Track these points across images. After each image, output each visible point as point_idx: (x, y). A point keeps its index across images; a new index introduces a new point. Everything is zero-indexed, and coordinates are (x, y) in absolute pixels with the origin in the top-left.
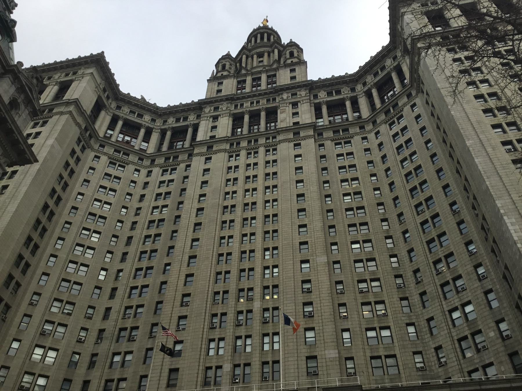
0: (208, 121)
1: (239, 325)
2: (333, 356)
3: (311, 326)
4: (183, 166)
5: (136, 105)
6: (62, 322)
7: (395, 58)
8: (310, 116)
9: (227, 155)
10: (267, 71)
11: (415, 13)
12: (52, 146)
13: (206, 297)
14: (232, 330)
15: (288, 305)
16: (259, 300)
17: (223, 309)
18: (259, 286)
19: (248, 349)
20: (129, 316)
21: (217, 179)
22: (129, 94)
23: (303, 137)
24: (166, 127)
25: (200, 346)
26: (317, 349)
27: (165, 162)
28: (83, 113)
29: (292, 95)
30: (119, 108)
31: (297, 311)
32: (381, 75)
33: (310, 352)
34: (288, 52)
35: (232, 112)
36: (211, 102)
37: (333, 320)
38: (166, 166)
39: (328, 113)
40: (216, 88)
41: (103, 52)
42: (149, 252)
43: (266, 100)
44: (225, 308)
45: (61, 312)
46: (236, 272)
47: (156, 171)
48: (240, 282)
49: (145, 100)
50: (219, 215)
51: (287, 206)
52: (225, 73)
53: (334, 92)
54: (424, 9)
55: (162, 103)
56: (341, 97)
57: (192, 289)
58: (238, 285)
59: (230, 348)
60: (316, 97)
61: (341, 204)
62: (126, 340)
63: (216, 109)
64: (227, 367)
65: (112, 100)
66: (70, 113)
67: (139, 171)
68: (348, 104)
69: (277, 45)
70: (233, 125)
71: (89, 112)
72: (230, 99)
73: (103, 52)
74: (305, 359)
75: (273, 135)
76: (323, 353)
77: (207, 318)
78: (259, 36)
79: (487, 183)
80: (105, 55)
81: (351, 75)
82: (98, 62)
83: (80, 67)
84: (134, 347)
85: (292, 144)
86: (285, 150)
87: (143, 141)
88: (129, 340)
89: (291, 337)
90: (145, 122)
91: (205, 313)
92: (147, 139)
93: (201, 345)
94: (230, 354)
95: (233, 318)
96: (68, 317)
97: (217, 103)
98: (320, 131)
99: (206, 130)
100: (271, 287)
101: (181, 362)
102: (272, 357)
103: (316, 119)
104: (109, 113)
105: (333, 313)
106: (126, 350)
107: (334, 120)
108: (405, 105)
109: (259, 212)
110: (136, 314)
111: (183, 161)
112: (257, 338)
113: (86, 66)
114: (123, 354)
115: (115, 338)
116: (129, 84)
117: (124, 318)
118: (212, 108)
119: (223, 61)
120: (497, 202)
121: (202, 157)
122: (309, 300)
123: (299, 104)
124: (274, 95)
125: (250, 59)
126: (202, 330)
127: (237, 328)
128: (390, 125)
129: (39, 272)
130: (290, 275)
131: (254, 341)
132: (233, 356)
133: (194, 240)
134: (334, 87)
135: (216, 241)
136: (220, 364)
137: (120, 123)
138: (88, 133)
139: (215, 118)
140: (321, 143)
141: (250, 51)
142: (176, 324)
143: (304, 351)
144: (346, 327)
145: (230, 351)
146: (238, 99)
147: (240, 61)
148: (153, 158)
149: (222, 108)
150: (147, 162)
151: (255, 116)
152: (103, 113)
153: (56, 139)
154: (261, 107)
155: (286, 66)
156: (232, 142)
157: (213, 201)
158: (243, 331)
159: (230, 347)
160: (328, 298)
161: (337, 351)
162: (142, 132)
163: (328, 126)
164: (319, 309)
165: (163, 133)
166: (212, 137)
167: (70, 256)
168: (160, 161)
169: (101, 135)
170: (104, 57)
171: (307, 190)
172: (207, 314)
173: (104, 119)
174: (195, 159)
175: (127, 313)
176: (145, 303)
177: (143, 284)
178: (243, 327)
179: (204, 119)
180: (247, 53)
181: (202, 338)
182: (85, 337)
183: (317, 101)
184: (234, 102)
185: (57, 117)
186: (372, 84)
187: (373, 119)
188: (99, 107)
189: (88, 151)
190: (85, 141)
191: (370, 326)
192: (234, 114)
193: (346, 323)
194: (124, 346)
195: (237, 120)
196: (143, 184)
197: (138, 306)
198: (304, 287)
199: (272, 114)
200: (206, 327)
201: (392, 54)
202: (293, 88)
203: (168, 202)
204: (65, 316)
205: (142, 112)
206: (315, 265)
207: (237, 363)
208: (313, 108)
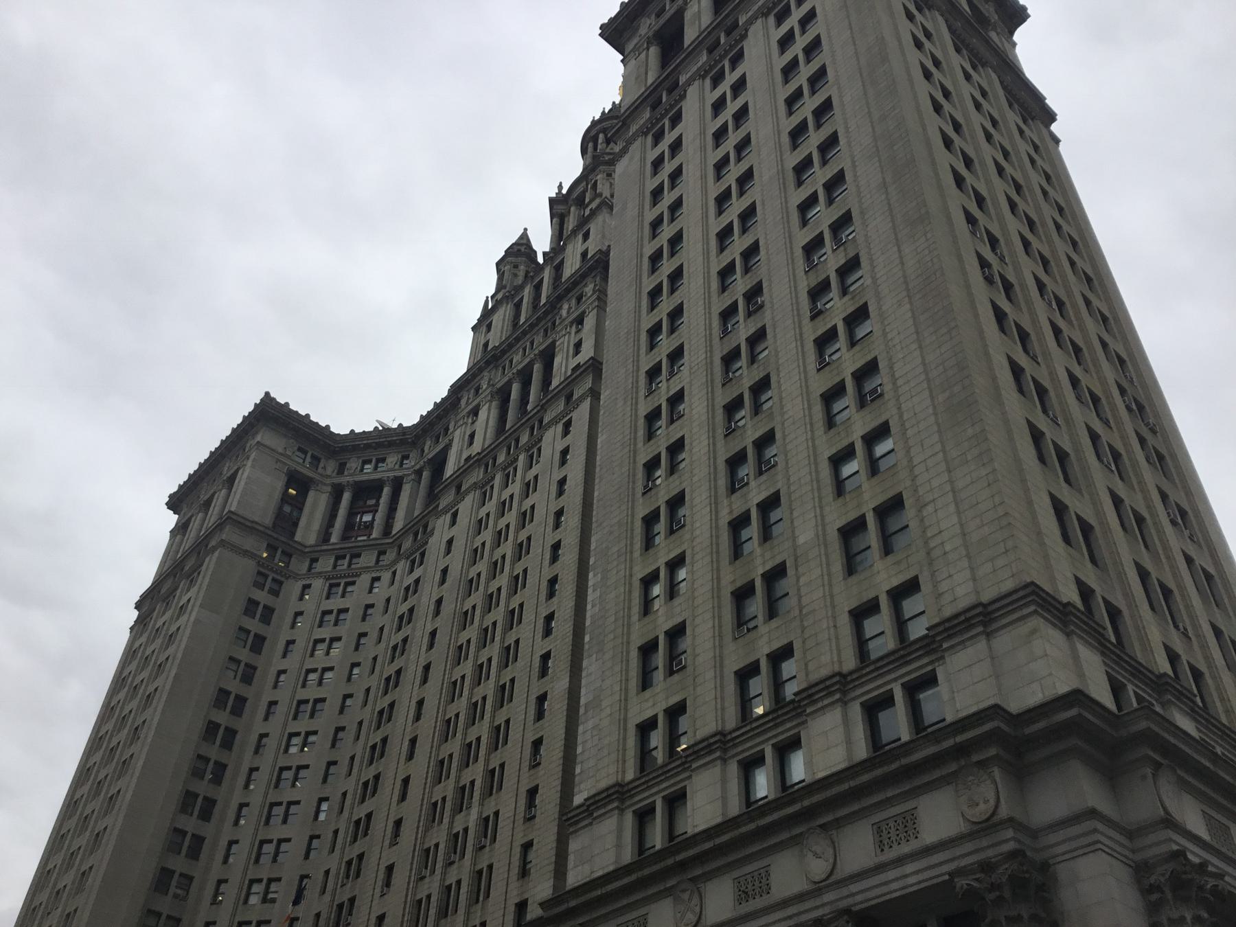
5: (368, 446)
22: (352, 431)
28: (252, 528)
30: (341, 469)
40: (482, 342)
41: (267, 394)
55: (410, 419)
66: (223, 543)
71: (268, 520)
73: (267, 394)
78: (591, 145)
82: (270, 414)
96: (271, 905)
129: (223, 843)
137: (347, 496)
139: (475, 412)
143: (515, 893)
148: (398, 543)
150: (391, 555)
152: (311, 494)
162: (386, 491)
170: (274, 399)
178: (455, 866)
192: (500, 390)
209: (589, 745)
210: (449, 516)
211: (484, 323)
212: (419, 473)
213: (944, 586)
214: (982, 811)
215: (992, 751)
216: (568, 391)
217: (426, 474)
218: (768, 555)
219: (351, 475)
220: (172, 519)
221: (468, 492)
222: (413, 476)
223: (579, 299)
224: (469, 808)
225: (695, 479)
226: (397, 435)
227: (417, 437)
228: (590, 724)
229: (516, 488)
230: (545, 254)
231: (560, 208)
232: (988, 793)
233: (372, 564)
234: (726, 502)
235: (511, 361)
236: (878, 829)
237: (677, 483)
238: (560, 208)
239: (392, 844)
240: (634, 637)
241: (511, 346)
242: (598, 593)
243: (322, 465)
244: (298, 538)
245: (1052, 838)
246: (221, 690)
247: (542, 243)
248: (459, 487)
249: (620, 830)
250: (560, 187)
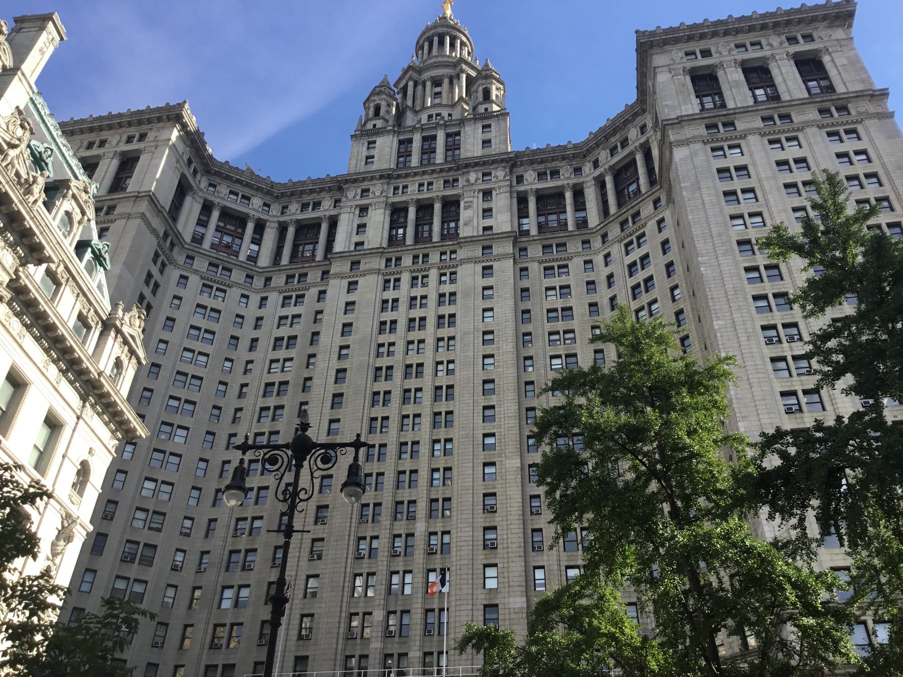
0: (352, 215)
1: (394, 555)
2: (519, 605)
3: (493, 561)
4: (313, 292)
6: (150, 542)
7: (643, 129)
8: (509, 218)
9: (381, 279)
10: (445, 126)
11: (674, 70)
13: (350, 512)
14: (385, 563)
15: (464, 530)
16: (424, 520)
17: (373, 531)
18: (425, 499)
19: (408, 590)
20: (242, 531)
21: (366, 321)
23: (498, 255)
25: (342, 584)
26: (499, 595)
27: (286, 283)
28: (160, 212)
29: (484, 175)
31: (475, 539)
32: (621, 154)
33: (490, 599)
34: (481, 88)
35: (391, 200)
36: (355, 181)
37: (522, 554)
38: (289, 291)
39: (538, 209)
40: (365, 153)
42: (267, 434)
43: (442, 182)
44: (376, 529)
45: (147, 527)
46: (392, 475)
47: (274, 298)
48: (399, 491)
49: (252, 173)
50: (369, 382)
51: (467, 377)
52: (379, 123)
53: (548, 172)
54: (689, 65)
56: (559, 183)
57: (330, 499)
58: (395, 495)
59: (382, 588)
60: (520, 180)
61: (546, 373)
62: (239, 569)
64: (378, 615)
65: (202, 175)
66: (143, 216)
67: (247, 297)
68: (568, 195)
69: (464, 67)
70: (391, 221)
72: (386, 176)
74: (482, 607)
75: (452, 248)
76: (506, 600)
77: (351, 543)
78: (436, 39)
79: (732, 393)
81: (576, 146)
83: (150, 126)
84: (251, 578)
85: (479, 268)
86: (469, 276)
87: (252, 242)
88: (243, 569)
89: (465, 577)
90: (254, 210)
91: (349, 536)
93: (344, 582)
94: (382, 597)
95: (387, 545)
97: (366, 183)
99: (349, 230)
100: (441, 501)
101: (317, 605)
102: (439, 603)
103: (520, 218)
104: (198, 199)
105: (522, 545)
106: (241, 583)
107: (547, 221)
108: (649, 218)
109: (427, 382)
110: (251, 529)
111: (315, 285)
112: (420, 575)
113: (161, 124)
114: (236, 588)
115: (224, 563)
117: (235, 536)
118: (359, 191)
119: (375, 98)
120: (740, 424)
121: (343, 280)
122: (492, 524)
123: (494, 193)
124: (455, 173)
125: (420, 87)
126: (344, 560)
127: (392, 559)
128: (627, 246)
130: (467, 484)
131: (416, 580)
132: (386, 600)
133: (331, 421)
134: (549, 165)
135: (364, 425)
136: (370, 610)
137: (216, 214)
138: (169, 241)
139: (364, 210)
140: (524, 265)
141: (420, 71)
142: (308, 550)
143: (482, 596)
144: (540, 564)
145: (383, 592)
146: (399, 177)
147: (404, 90)
148: (268, 275)
149: (374, 193)
151: (425, 208)
152: (188, 200)
153: (124, 264)
154: (435, 195)
155: (476, 117)
156: (388, 256)
157: (361, 359)
158: (401, 563)
159: (383, 587)
160: (517, 522)
161: (525, 599)
162: (250, 226)
163: (535, 238)
164: (505, 537)
165: (282, 229)
166: (359, 244)
167: (154, 442)
168: (279, 280)
169: (188, 238)
171: (498, 348)
172: (352, 538)
174: (333, 282)
175: (239, 527)
176: (264, 514)
177: (260, 485)
178: (401, 558)
179: (345, 209)
180: (415, 76)
181: (345, 572)
182: (183, 562)
183: (521, 188)
184: (393, 181)
185: (122, 222)
186: (607, 167)
187: (603, 232)
188: (183, 190)
189: (169, 269)
190: (165, 255)
191: (572, 564)
192: (393, 204)
193: (540, 558)
194: (238, 577)
195: (397, 213)
196: (254, 321)
197: (254, 518)
198: (486, 503)
199: (451, 206)
200: (350, 556)
201: (639, 121)
202: (484, 164)
203: (292, 353)
204: (152, 532)
205: (247, 192)
206: (504, 470)
207: (392, 609)
208: (515, 201)
222: (276, 225)
226: (267, 185)
227: (283, 195)
233: (242, 281)
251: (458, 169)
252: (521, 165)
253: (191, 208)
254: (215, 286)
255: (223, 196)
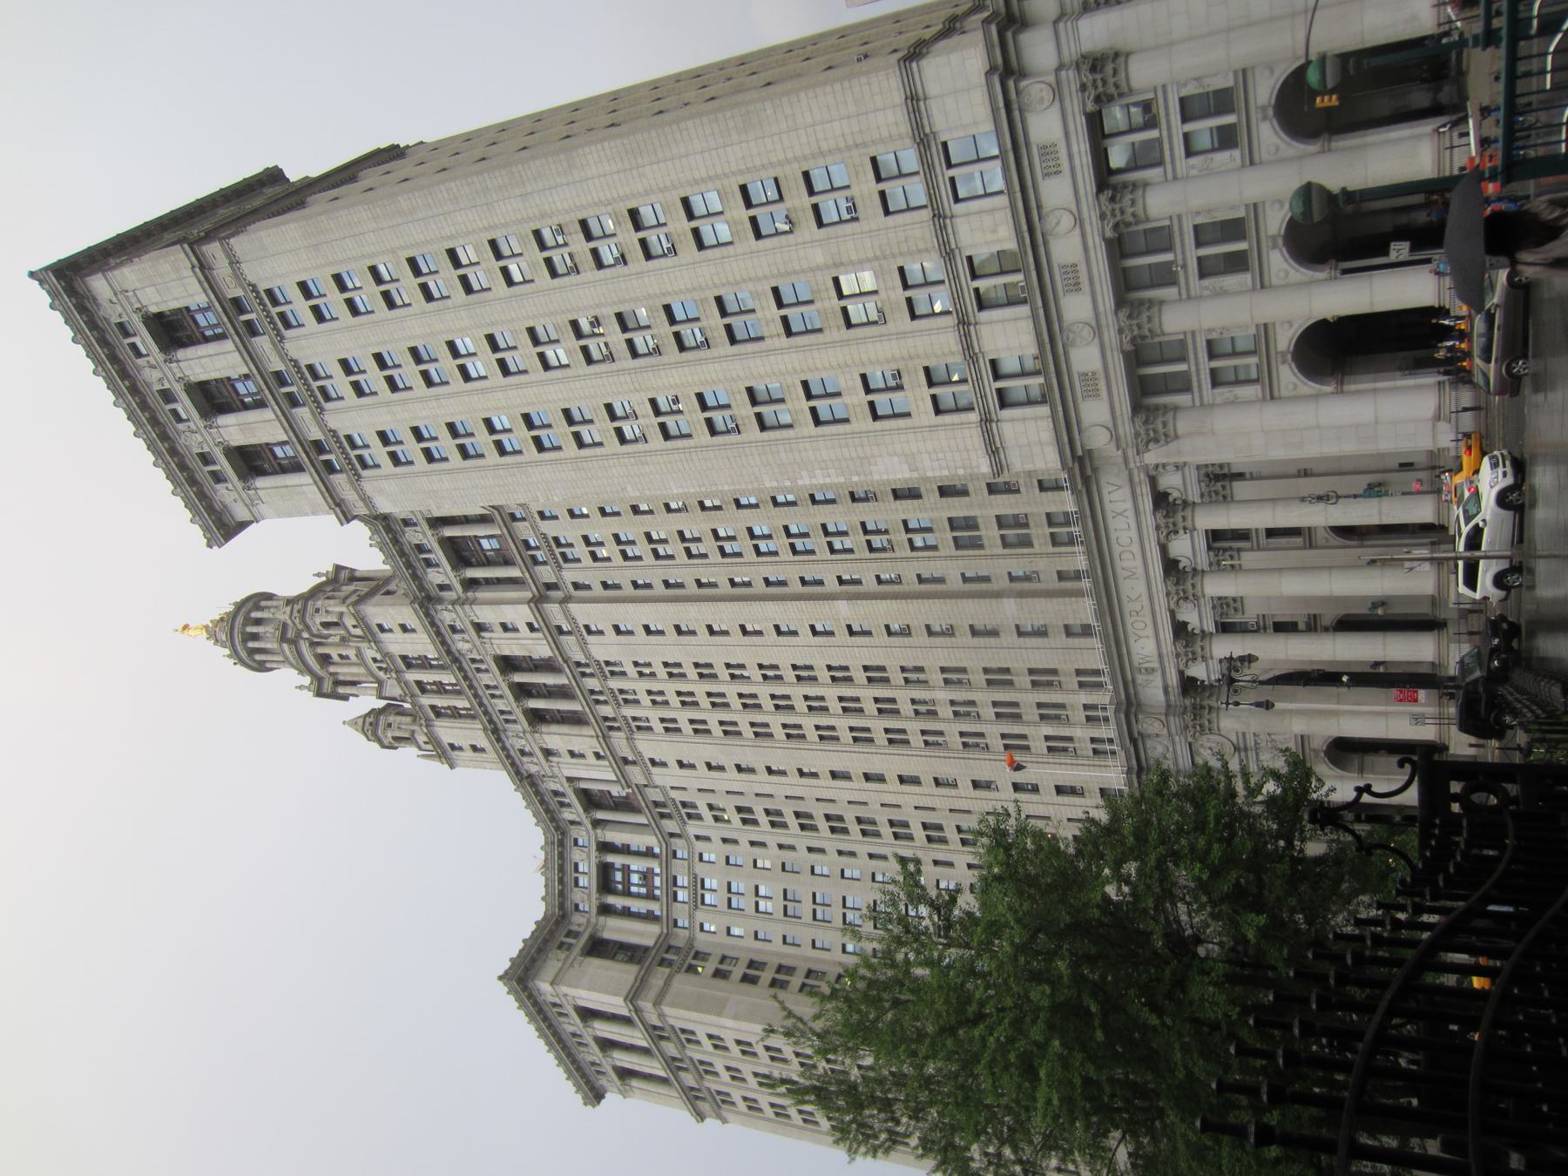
5: (561, 881)
9: (638, 735)
12: (736, 1017)
24: (587, 822)
36: (513, 764)
40: (471, 753)
41: (500, 978)
63: (523, 753)
68: (449, 532)
71: (633, 969)
73: (500, 978)
78: (258, 657)
80: (501, 973)
82: (521, 976)
92: (625, 850)
98: (542, 589)
116: (528, 908)
118: (525, 759)
134: (412, 558)
137: (611, 900)
139: (548, 753)
152: (607, 935)
153: (719, 1014)
168: (670, 826)
173: (619, 930)
188: (599, 948)
189: (699, 946)
202: (439, 634)
205: (569, 868)
209: (943, 463)
210: (655, 770)
211: (444, 753)
212: (597, 823)
213: (885, 133)
214: (1047, 95)
215: (1011, 83)
216: (555, 632)
217: (600, 815)
218: (824, 295)
219: (589, 895)
220: (612, 1099)
221: (633, 748)
222: (599, 831)
223: (453, 629)
224: (933, 702)
225: (741, 374)
227: (557, 828)
228: (927, 463)
229: (641, 687)
230: (380, 697)
231: (327, 686)
232: (1035, 90)
234: (768, 342)
235: (502, 712)
236: (1047, 175)
237: (738, 397)
238: (327, 686)
239: (955, 785)
240: (864, 428)
241: (486, 713)
242: (818, 472)
243: (575, 928)
244: (650, 942)
245: (1066, 52)
246: (801, 990)
247: (366, 702)
248: (626, 761)
249: (1012, 420)
250: (300, 687)
251: (456, 660)
252: (421, 588)
253: (616, 930)
254: (700, 891)
255: (585, 894)
